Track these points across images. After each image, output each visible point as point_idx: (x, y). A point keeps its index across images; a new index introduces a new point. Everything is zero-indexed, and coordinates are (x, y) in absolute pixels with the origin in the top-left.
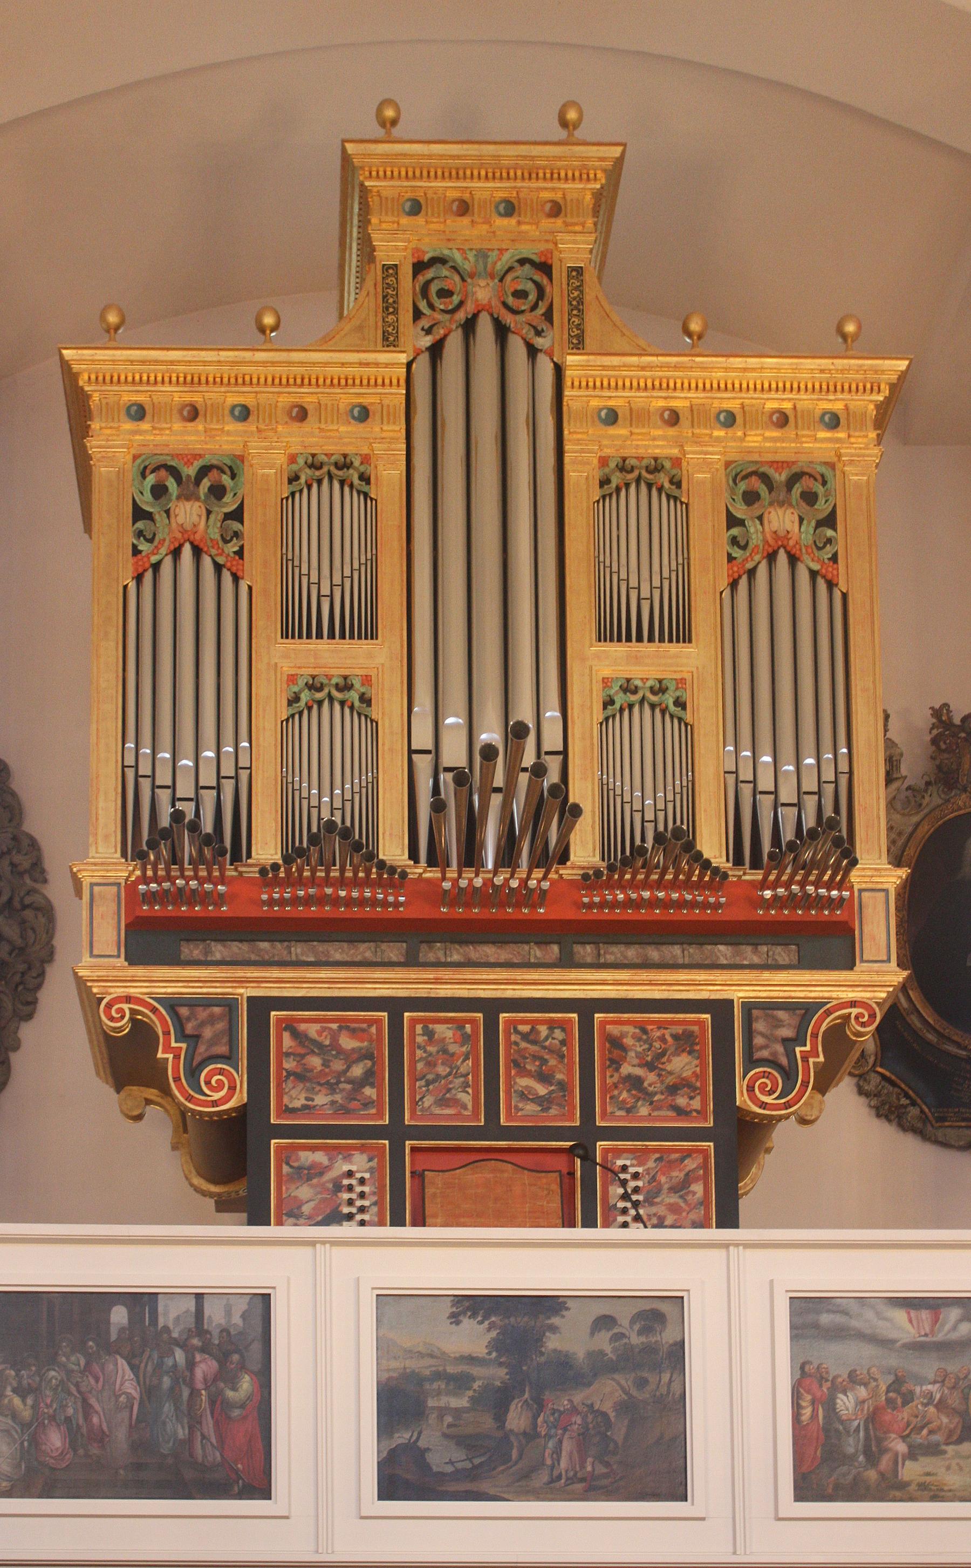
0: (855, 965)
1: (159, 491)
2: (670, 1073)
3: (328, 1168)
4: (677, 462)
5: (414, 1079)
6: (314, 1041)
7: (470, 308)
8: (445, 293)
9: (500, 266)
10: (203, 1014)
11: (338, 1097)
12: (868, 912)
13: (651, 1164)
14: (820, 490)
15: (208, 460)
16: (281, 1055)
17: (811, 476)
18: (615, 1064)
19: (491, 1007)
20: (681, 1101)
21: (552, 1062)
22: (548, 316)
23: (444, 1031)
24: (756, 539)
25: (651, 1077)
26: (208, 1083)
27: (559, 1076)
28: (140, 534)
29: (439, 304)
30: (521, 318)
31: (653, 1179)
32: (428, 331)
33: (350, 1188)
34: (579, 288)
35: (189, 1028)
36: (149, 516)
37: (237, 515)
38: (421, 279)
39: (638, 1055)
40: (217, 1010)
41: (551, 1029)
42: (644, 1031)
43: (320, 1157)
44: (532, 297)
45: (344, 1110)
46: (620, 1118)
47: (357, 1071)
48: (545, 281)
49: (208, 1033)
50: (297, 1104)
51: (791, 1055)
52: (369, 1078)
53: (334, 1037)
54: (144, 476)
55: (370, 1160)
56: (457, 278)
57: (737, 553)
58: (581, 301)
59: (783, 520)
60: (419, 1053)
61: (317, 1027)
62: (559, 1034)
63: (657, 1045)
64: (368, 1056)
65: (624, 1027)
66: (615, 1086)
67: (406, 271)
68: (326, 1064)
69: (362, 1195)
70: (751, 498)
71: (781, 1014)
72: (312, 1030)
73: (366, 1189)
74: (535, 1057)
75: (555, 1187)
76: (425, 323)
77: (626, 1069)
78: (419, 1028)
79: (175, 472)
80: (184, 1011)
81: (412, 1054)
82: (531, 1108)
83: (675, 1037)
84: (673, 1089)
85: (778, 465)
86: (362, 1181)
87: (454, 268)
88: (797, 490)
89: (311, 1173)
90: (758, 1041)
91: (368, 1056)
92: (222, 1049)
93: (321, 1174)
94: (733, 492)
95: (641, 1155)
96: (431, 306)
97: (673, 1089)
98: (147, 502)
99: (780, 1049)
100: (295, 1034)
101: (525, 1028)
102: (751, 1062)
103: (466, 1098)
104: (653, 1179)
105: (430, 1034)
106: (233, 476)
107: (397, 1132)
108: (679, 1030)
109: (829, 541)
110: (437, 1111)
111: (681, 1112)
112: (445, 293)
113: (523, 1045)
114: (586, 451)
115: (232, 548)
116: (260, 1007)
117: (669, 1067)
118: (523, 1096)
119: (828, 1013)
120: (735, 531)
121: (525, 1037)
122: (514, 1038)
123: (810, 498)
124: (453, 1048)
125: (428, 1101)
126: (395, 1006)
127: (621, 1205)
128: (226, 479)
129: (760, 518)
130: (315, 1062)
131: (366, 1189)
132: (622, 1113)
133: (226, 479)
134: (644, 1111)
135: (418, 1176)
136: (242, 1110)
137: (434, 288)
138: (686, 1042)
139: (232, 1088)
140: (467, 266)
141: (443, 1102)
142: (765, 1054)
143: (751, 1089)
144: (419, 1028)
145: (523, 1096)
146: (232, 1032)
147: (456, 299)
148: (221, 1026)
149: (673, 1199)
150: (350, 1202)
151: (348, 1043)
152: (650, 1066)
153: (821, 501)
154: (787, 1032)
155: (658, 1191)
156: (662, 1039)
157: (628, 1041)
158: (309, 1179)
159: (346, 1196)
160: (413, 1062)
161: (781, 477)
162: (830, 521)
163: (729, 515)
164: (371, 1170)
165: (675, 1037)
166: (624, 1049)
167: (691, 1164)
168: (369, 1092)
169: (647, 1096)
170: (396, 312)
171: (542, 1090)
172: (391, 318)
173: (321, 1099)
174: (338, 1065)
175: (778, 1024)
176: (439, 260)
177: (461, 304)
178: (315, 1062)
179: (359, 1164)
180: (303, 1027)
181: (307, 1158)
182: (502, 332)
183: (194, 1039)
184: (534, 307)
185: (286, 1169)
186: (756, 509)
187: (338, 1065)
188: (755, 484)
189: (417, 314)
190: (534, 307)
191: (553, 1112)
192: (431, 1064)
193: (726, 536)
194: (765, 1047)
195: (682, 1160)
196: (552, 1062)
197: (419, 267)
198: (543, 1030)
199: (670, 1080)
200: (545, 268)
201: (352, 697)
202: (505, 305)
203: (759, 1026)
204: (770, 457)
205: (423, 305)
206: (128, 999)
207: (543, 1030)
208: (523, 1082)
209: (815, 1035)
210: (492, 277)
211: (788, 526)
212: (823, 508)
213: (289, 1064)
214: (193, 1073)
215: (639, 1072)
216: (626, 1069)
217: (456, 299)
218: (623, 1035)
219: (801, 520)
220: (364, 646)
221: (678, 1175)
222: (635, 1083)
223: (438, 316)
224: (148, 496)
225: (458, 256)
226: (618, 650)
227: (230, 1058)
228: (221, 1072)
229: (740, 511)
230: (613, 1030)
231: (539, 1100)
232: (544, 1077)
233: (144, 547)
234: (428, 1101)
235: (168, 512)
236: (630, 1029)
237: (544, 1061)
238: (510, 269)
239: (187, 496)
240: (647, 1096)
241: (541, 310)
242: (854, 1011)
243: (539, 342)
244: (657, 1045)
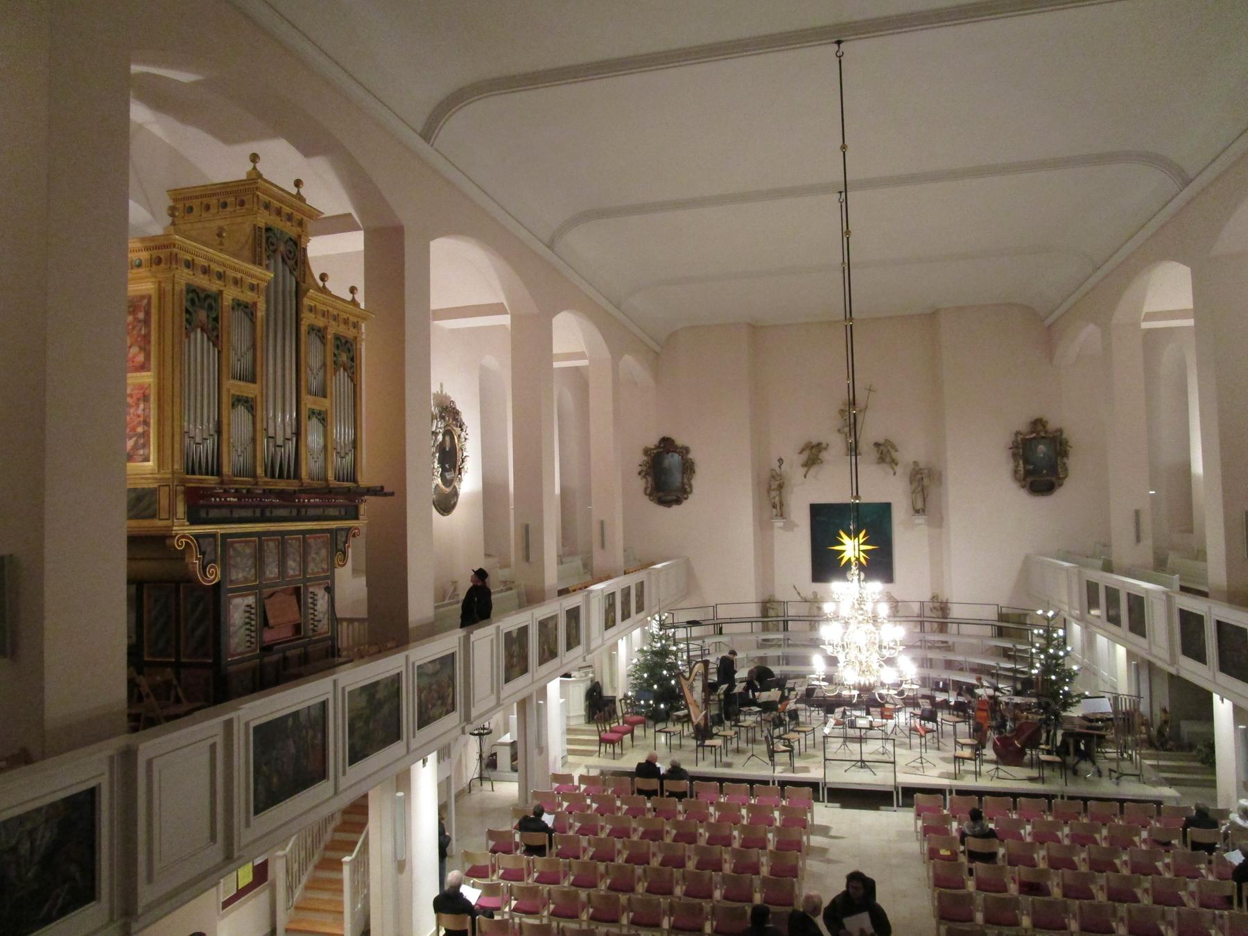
1: (193, 302)
70: (338, 347)
114: (308, 319)
116: (225, 536)
136: (218, 584)
183: (203, 553)
201: (249, 404)
206: (183, 537)
214: (204, 568)
220: (252, 385)
227: (214, 562)
239: (202, 308)
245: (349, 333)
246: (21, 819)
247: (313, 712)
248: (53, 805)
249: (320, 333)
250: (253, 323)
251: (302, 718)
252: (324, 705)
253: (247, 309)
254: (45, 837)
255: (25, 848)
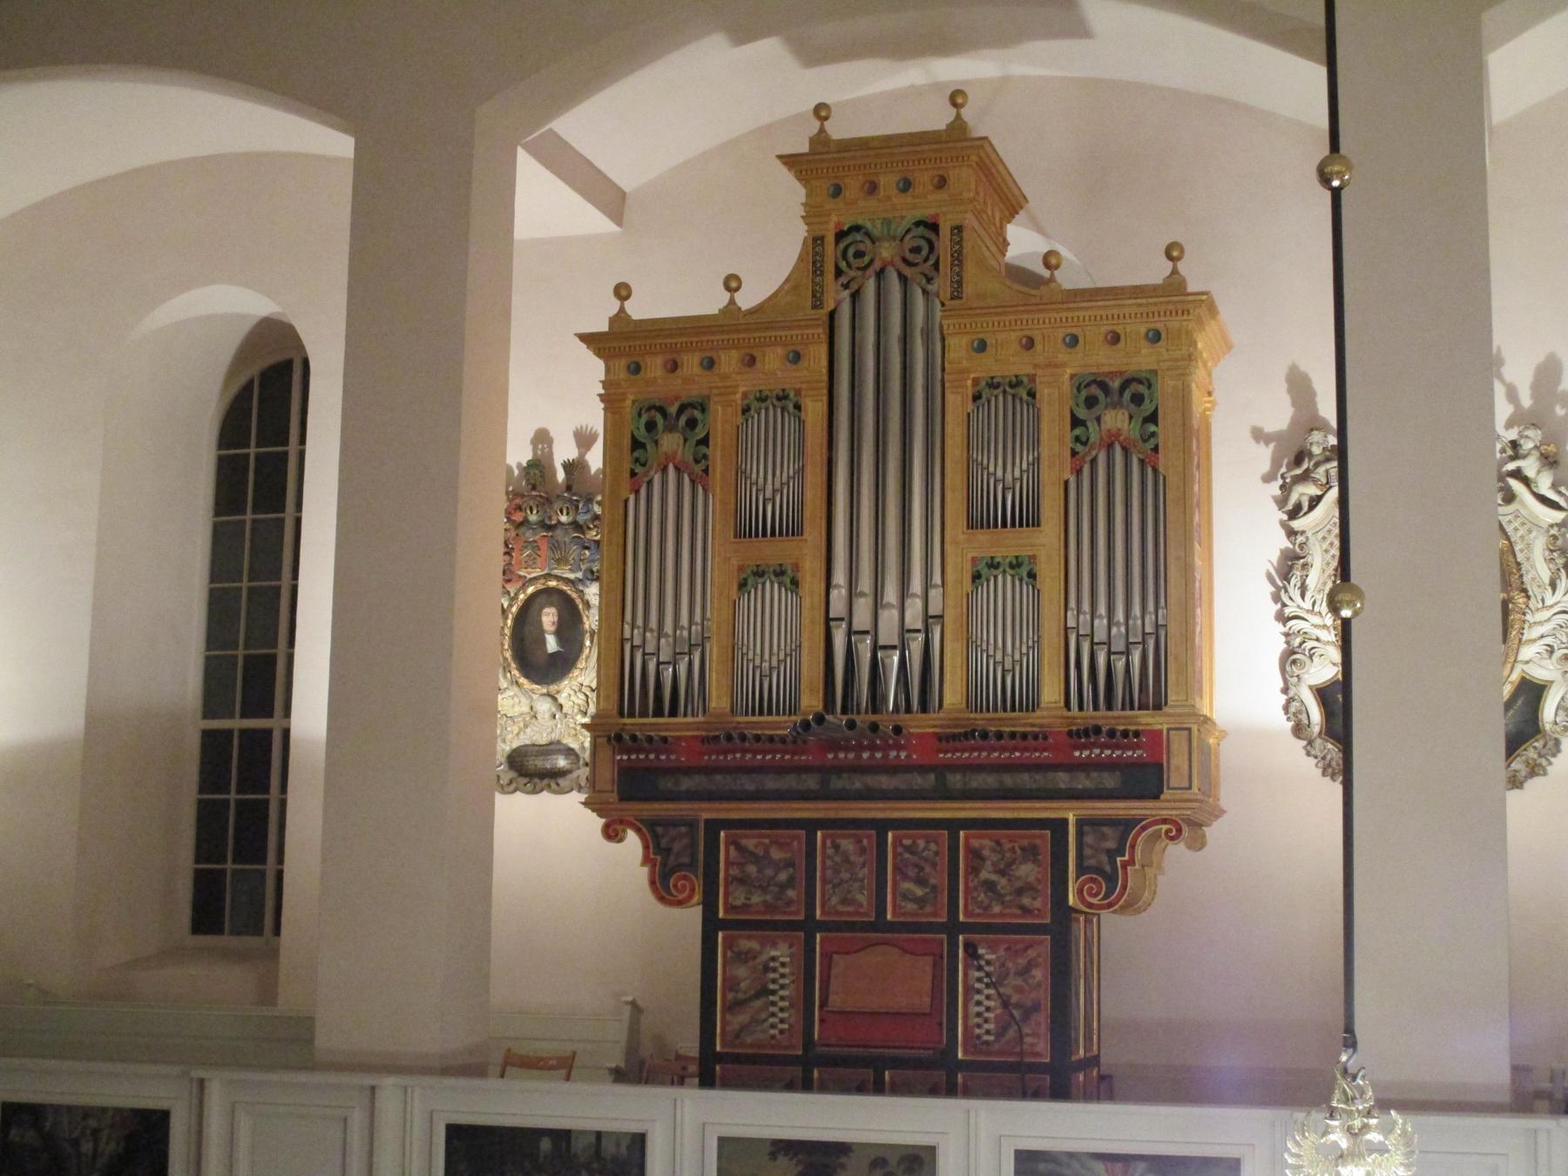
0: (1161, 792)
2: (1018, 878)
3: (760, 953)
4: (1032, 378)
5: (824, 881)
6: (752, 854)
7: (877, 265)
8: (859, 254)
9: (900, 231)
10: (673, 832)
11: (768, 898)
12: (1174, 747)
13: (1002, 952)
14: (1146, 392)
15: (684, 400)
16: (728, 864)
17: (1140, 382)
18: (973, 870)
19: (882, 826)
20: (1026, 901)
21: (928, 869)
22: (936, 266)
23: (847, 845)
24: (1094, 437)
25: (1003, 881)
26: (675, 886)
27: (933, 881)
28: (637, 460)
29: (855, 263)
30: (918, 269)
31: (1003, 965)
32: (846, 286)
33: (775, 970)
34: (960, 243)
35: (664, 842)
36: (642, 446)
37: (704, 441)
38: (842, 246)
39: (994, 864)
40: (683, 829)
41: (928, 842)
42: (998, 843)
43: (755, 945)
44: (925, 252)
45: (769, 908)
46: (979, 915)
47: (783, 876)
48: (932, 236)
49: (676, 847)
50: (738, 903)
51: (1113, 863)
52: (791, 882)
53: (767, 852)
54: (640, 415)
55: (791, 946)
56: (868, 242)
57: (1079, 448)
58: (960, 253)
59: (1116, 420)
60: (829, 863)
61: (754, 841)
62: (933, 846)
63: (1008, 855)
64: (790, 864)
65: (984, 842)
66: (976, 889)
67: (830, 239)
68: (760, 871)
69: (783, 976)
70: (1091, 402)
71: (1105, 829)
72: (750, 843)
73: (786, 970)
74: (916, 866)
75: (929, 969)
76: (843, 280)
77: (984, 875)
78: (829, 843)
79: (662, 410)
80: (660, 830)
81: (823, 862)
82: (910, 906)
83: (1023, 849)
84: (1019, 892)
85: (1112, 374)
86: (783, 965)
87: (867, 234)
88: (1127, 395)
89: (745, 957)
90: (1088, 852)
91: (790, 864)
92: (686, 860)
93: (755, 958)
94: (1076, 397)
95: (993, 948)
96: (849, 265)
97: (1019, 892)
98: (642, 434)
99: (1104, 858)
100: (739, 847)
101: (907, 842)
102: (1081, 870)
103: (862, 898)
104: (1003, 965)
105: (836, 847)
106: (703, 410)
107: (809, 926)
108: (1025, 842)
109: (1153, 434)
110: (841, 908)
111: (1026, 911)
112: (859, 254)
113: (907, 855)
115: (702, 466)
116: (713, 827)
117: (1018, 873)
118: (905, 897)
119: (1144, 828)
120: (1078, 431)
121: (908, 849)
122: (900, 850)
123: (1138, 399)
124: (852, 858)
125: (834, 900)
126: (811, 826)
127: (977, 985)
128: (697, 414)
129: (1098, 420)
130: (752, 869)
131: (786, 970)
132: (978, 911)
133: (697, 414)
134: (997, 909)
135: (827, 957)
137: (851, 252)
138: (1031, 853)
139: (693, 890)
140: (876, 232)
141: (844, 901)
142: (1092, 862)
143: (1080, 892)
144: (829, 843)
145: (905, 897)
146: (693, 845)
147: (867, 259)
148: (685, 841)
149: (1019, 981)
150: (774, 981)
151: (776, 854)
152: (1002, 873)
153: (1147, 401)
154: (1111, 844)
155: (1007, 975)
156: (1013, 850)
157: (986, 852)
158: (746, 961)
159: (772, 976)
160: (824, 869)
161: (1115, 384)
162: (1153, 418)
163: (1073, 415)
164: (791, 956)
165: (1023, 849)
166: (983, 859)
167: (1032, 953)
168: (791, 893)
169: (1000, 897)
170: (822, 274)
171: (919, 892)
172: (818, 279)
173: (756, 899)
174: (769, 872)
175: (1104, 837)
176: (856, 228)
177: (872, 261)
178: (752, 869)
179: (781, 952)
180: (744, 842)
181: (746, 944)
182: (903, 279)
184: (926, 260)
185: (729, 954)
186: (1096, 411)
187: (769, 872)
188: (1095, 391)
189: (839, 273)
190: (926, 260)
191: (928, 909)
192: (837, 872)
193: (1069, 436)
194: (1092, 857)
195: (1026, 949)
196: (928, 869)
197: (840, 236)
198: (921, 843)
199: (1018, 884)
200: (934, 227)
202: (905, 260)
203: (1089, 839)
204: (1106, 369)
205: (843, 265)
207: (921, 843)
208: (907, 886)
209: (1133, 847)
210: (894, 238)
211: (1119, 425)
212: (1147, 407)
213: (734, 871)
215: (994, 877)
216: (984, 875)
217: (867, 259)
218: (982, 847)
219: (1131, 417)
221: (1022, 961)
222: (990, 886)
223: (852, 273)
224: (642, 428)
225: (869, 225)
226: (982, 536)
227: (692, 866)
228: (685, 877)
229: (1082, 413)
230: (975, 843)
231: (916, 900)
232: (921, 882)
233: (638, 469)
234: (834, 900)
235: (656, 442)
236: (987, 842)
237: (922, 869)
238: (908, 231)
239: (670, 429)
240: (1000, 897)
241: (931, 262)
242: (1165, 827)
243: (929, 287)
244: (1008, 855)
245: (1142, 359)
246: (87, 1112)
247: (609, 1148)
248: (118, 1110)
249: (1021, 390)
250: (801, 423)
251: (578, 1146)
252: (639, 1141)
253: (787, 401)
254: (110, 1147)
255: (87, 1147)
